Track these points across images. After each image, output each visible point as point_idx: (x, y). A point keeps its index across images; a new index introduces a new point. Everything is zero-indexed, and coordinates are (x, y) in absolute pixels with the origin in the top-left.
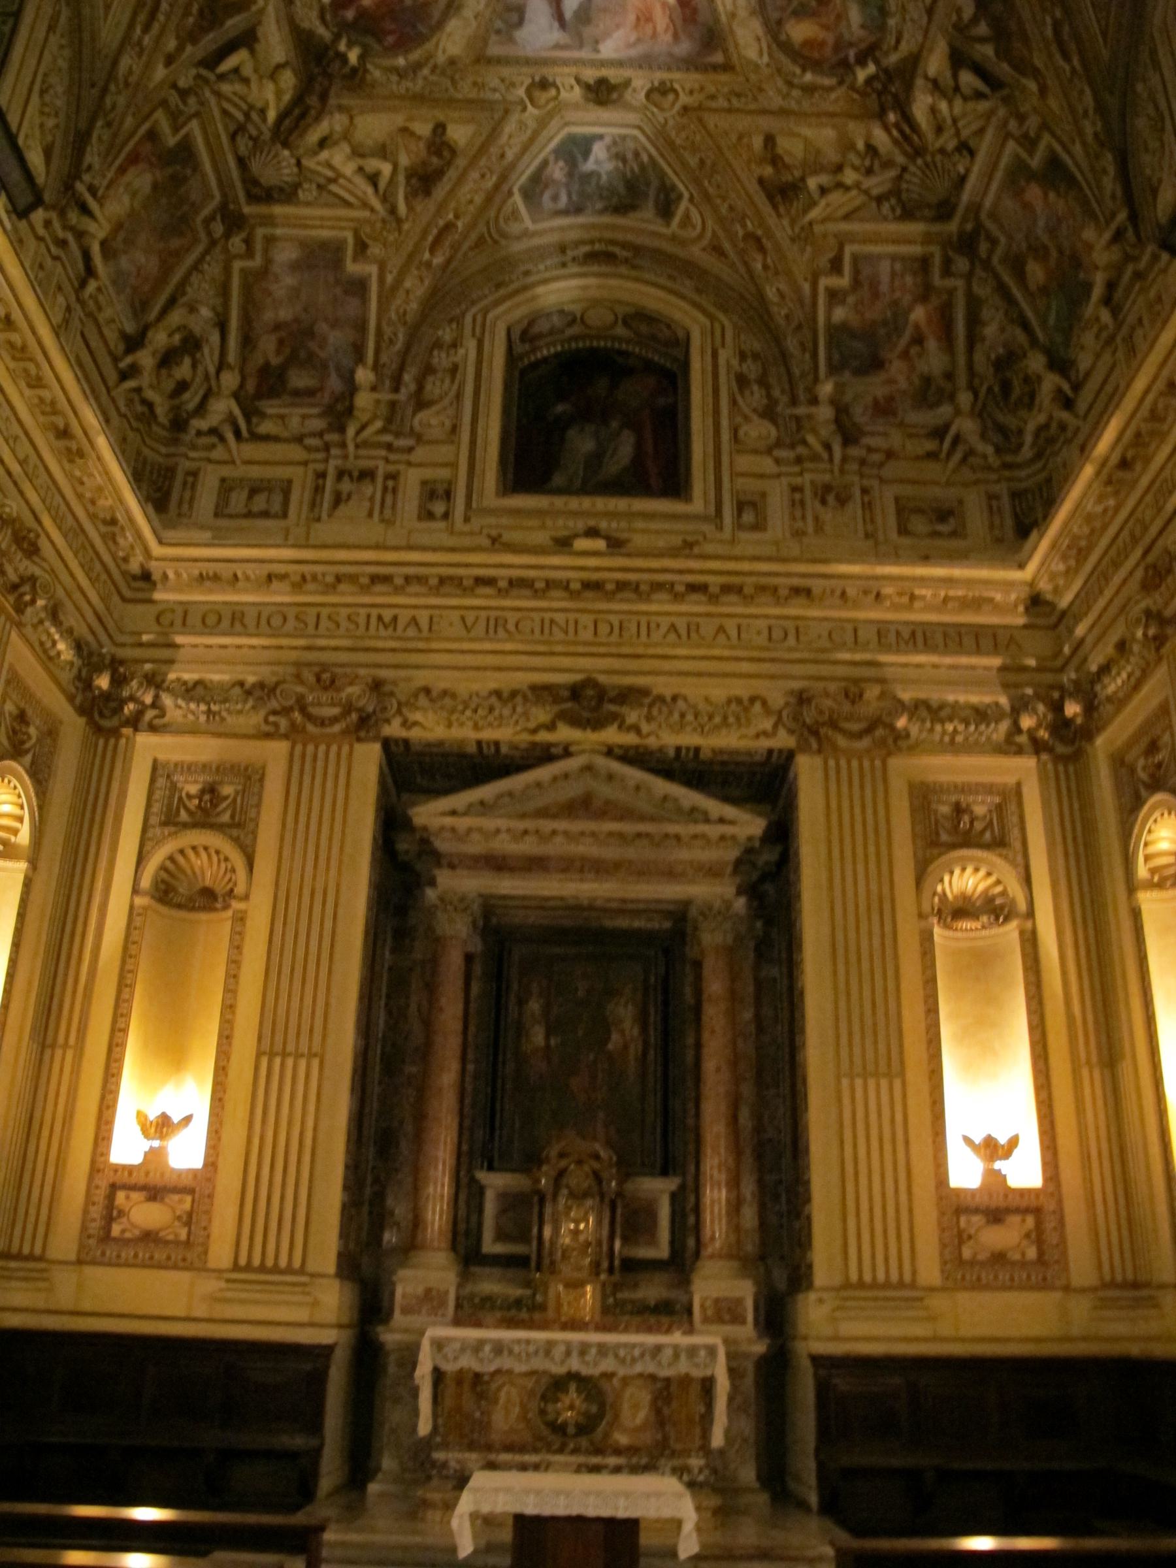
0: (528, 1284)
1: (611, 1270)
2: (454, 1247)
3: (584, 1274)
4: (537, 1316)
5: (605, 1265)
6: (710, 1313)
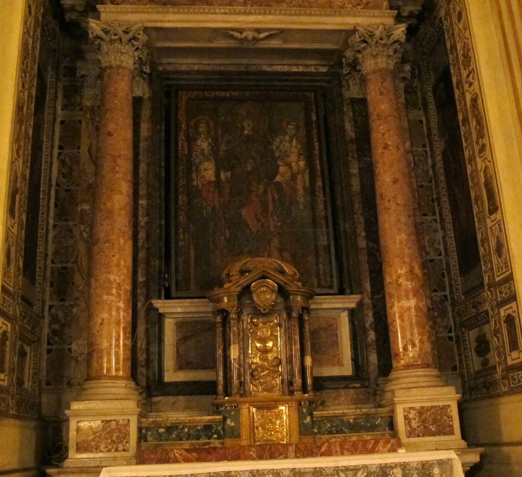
0: (216, 409)
1: (304, 389)
2: (134, 376)
3: (276, 394)
4: (229, 442)
5: (298, 381)
6: (414, 424)
